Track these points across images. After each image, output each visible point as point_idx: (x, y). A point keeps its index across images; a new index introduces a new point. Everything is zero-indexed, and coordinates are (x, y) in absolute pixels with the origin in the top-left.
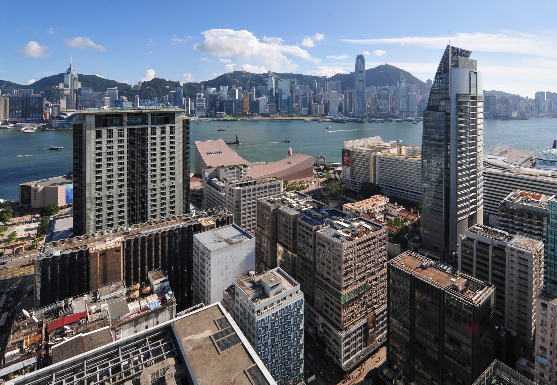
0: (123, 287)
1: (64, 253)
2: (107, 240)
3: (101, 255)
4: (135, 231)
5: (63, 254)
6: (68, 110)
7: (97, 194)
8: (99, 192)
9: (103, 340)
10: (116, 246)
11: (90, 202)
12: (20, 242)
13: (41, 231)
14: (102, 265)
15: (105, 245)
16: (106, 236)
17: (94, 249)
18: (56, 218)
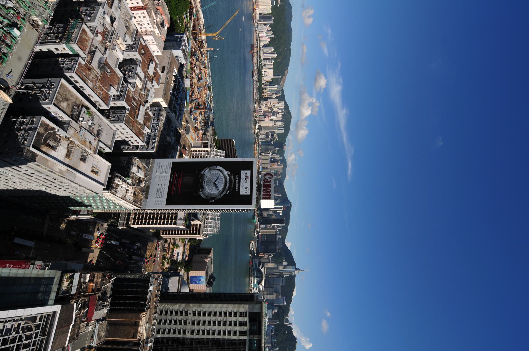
0: (99, 342)
1: (149, 294)
2: (148, 325)
3: (136, 322)
4: (146, 349)
5: (148, 293)
6: (266, 269)
7: (191, 312)
8: (192, 314)
9: (57, 343)
10: (138, 334)
11: (185, 307)
12: (171, 250)
13: (174, 263)
14: (127, 322)
15: (144, 323)
16: (151, 323)
17: (143, 316)
18: (181, 277)
